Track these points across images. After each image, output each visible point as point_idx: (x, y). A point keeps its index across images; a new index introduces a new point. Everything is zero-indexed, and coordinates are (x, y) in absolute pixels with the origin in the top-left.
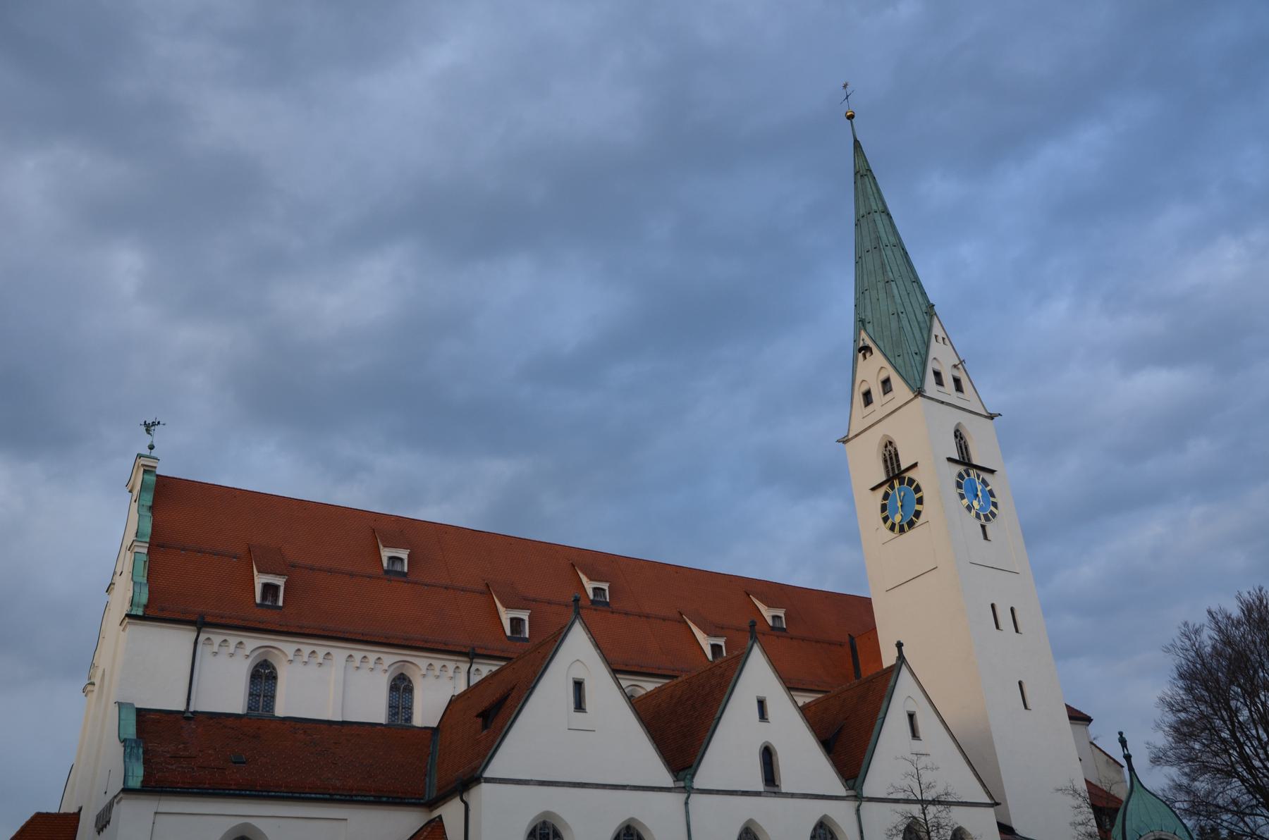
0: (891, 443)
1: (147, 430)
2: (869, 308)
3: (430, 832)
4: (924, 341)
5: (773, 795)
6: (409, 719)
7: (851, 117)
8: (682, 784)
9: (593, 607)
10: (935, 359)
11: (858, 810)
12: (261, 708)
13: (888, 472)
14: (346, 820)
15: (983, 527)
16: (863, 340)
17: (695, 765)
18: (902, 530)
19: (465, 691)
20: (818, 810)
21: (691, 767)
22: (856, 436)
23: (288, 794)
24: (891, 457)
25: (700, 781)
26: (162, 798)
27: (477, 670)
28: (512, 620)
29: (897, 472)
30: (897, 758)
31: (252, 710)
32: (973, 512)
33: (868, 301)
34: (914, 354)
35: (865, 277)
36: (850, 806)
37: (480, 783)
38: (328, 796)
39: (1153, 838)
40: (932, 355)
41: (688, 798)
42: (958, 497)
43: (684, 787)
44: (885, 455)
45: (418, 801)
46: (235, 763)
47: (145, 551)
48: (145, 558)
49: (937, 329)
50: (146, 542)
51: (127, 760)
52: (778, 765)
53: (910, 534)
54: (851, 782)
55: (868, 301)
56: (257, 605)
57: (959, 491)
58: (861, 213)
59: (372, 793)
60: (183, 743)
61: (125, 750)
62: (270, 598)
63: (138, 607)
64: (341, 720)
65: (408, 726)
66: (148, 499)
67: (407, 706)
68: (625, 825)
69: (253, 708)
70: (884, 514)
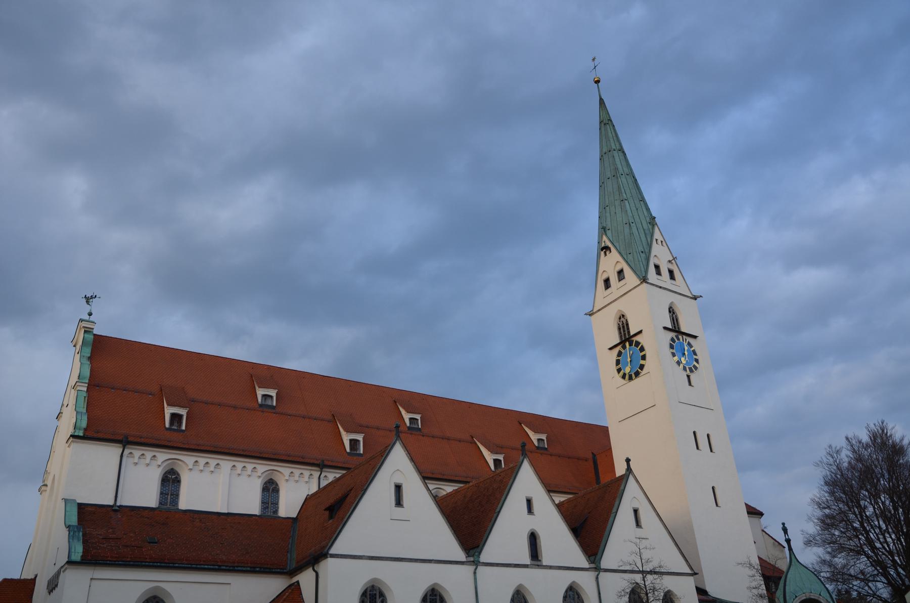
0: (623, 316)
1: (87, 302)
2: (609, 219)
3: (291, 592)
4: (648, 243)
5: (537, 567)
6: (276, 511)
7: (597, 82)
8: (472, 559)
9: (409, 432)
10: (655, 256)
11: (597, 578)
12: (169, 504)
13: (621, 337)
14: (230, 584)
15: (688, 376)
16: (604, 242)
17: (481, 546)
18: (631, 378)
19: (316, 491)
20: (569, 578)
21: (478, 547)
22: (599, 310)
23: (188, 566)
24: (623, 326)
25: (485, 557)
26: (97, 568)
27: (326, 476)
28: (351, 440)
29: (627, 337)
30: (625, 541)
31: (162, 505)
33: (608, 214)
34: (641, 253)
35: (607, 197)
36: (591, 575)
37: (327, 557)
38: (217, 567)
39: (805, 598)
40: (653, 253)
41: (476, 569)
43: (473, 561)
44: (619, 324)
45: (282, 571)
46: (149, 543)
47: (85, 389)
48: (85, 394)
49: (657, 235)
50: (86, 383)
51: (71, 540)
52: (540, 545)
53: (636, 381)
54: (592, 558)
55: (608, 214)
56: (167, 429)
57: (671, 350)
58: (604, 151)
59: (249, 565)
60: (112, 529)
61: (69, 533)
62: (176, 424)
63: (80, 430)
64: (227, 512)
65: (276, 517)
66: (87, 352)
67: (274, 502)
68: (431, 588)
69: (163, 503)
70: (618, 367)
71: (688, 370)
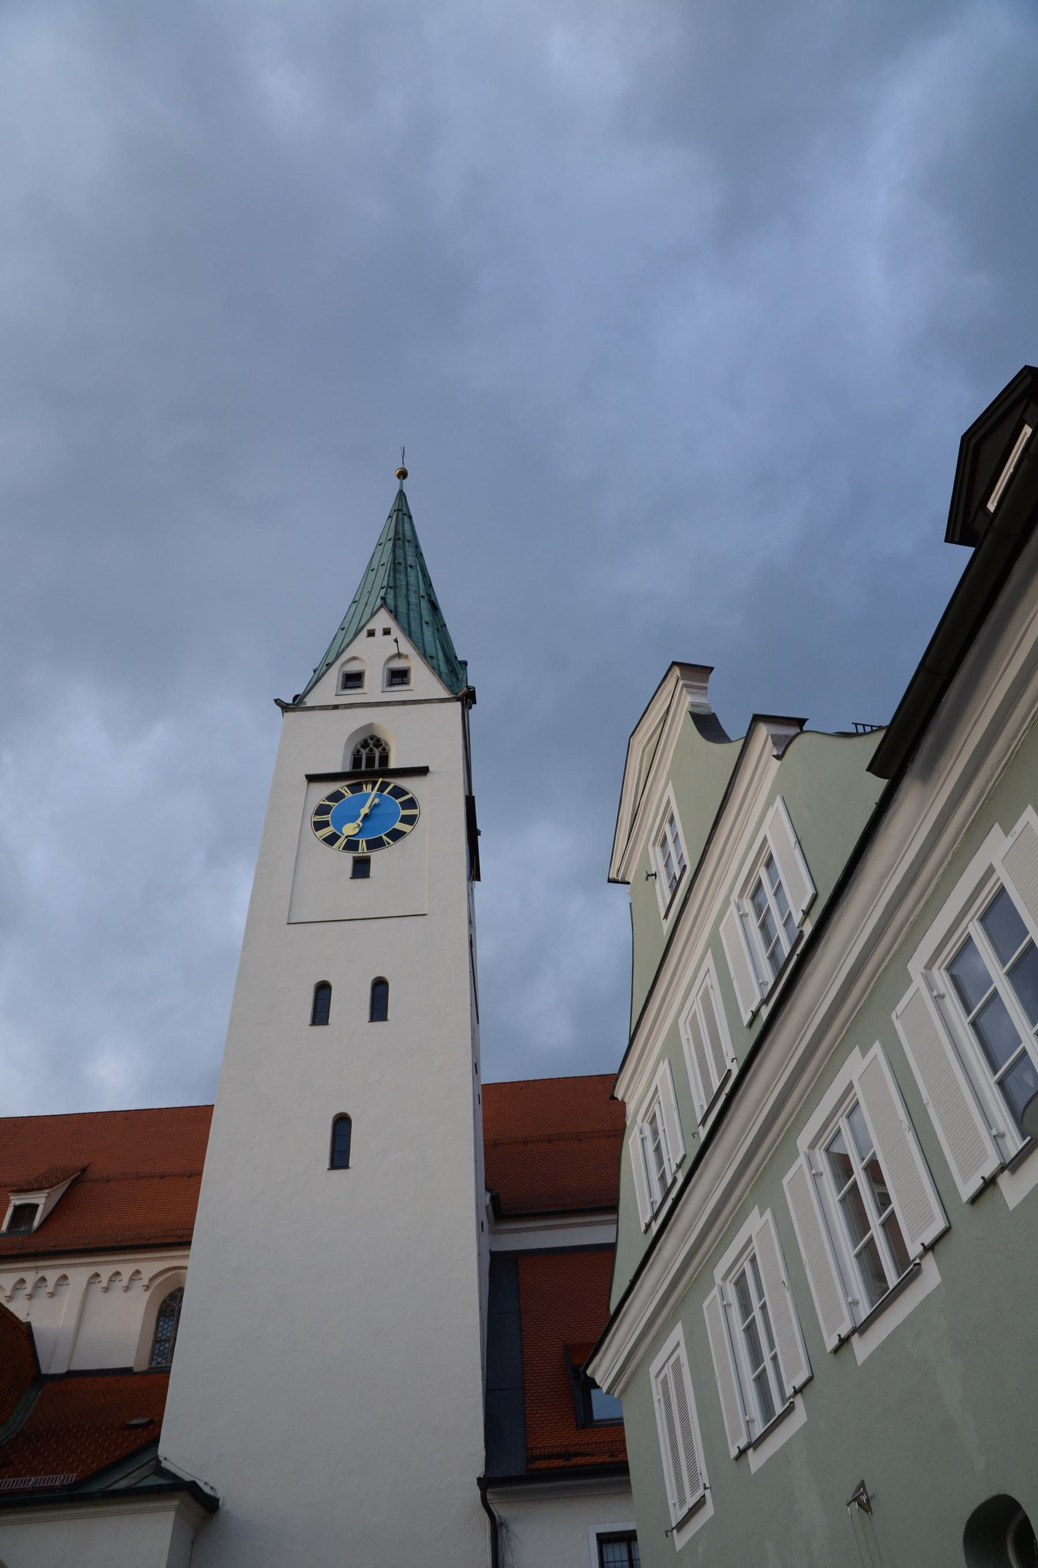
10: (354, 658)
32: (341, 842)
42: (309, 827)
71: (363, 845)
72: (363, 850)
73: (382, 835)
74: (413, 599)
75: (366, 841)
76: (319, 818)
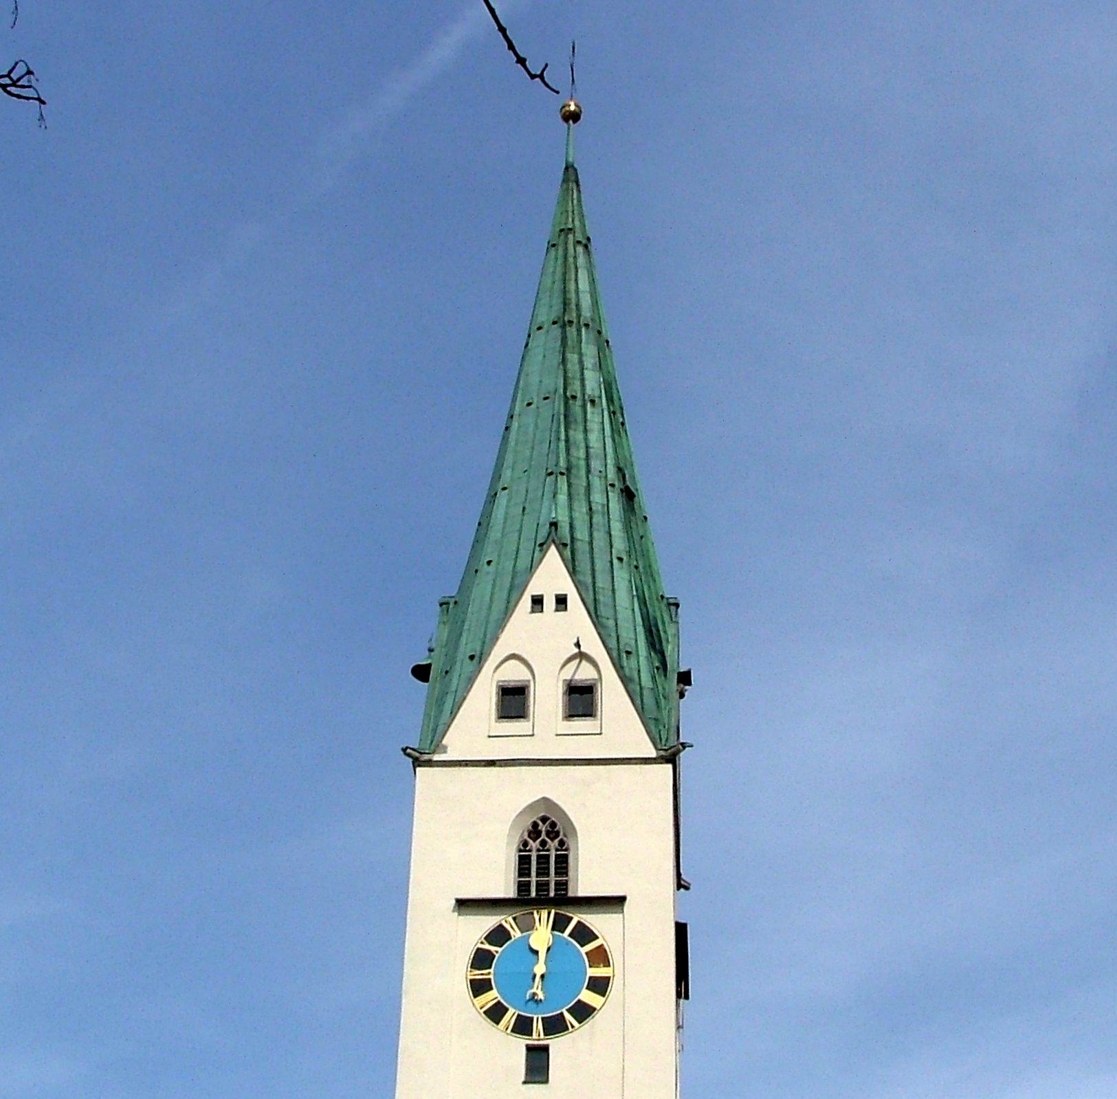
10: (513, 656)
32: (509, 1018)
71: (538, 1027)
72: (539, 1035)
73: (564, 1011)
74: (598, 498)
75: (543, 1019)
76: (478, 974)
